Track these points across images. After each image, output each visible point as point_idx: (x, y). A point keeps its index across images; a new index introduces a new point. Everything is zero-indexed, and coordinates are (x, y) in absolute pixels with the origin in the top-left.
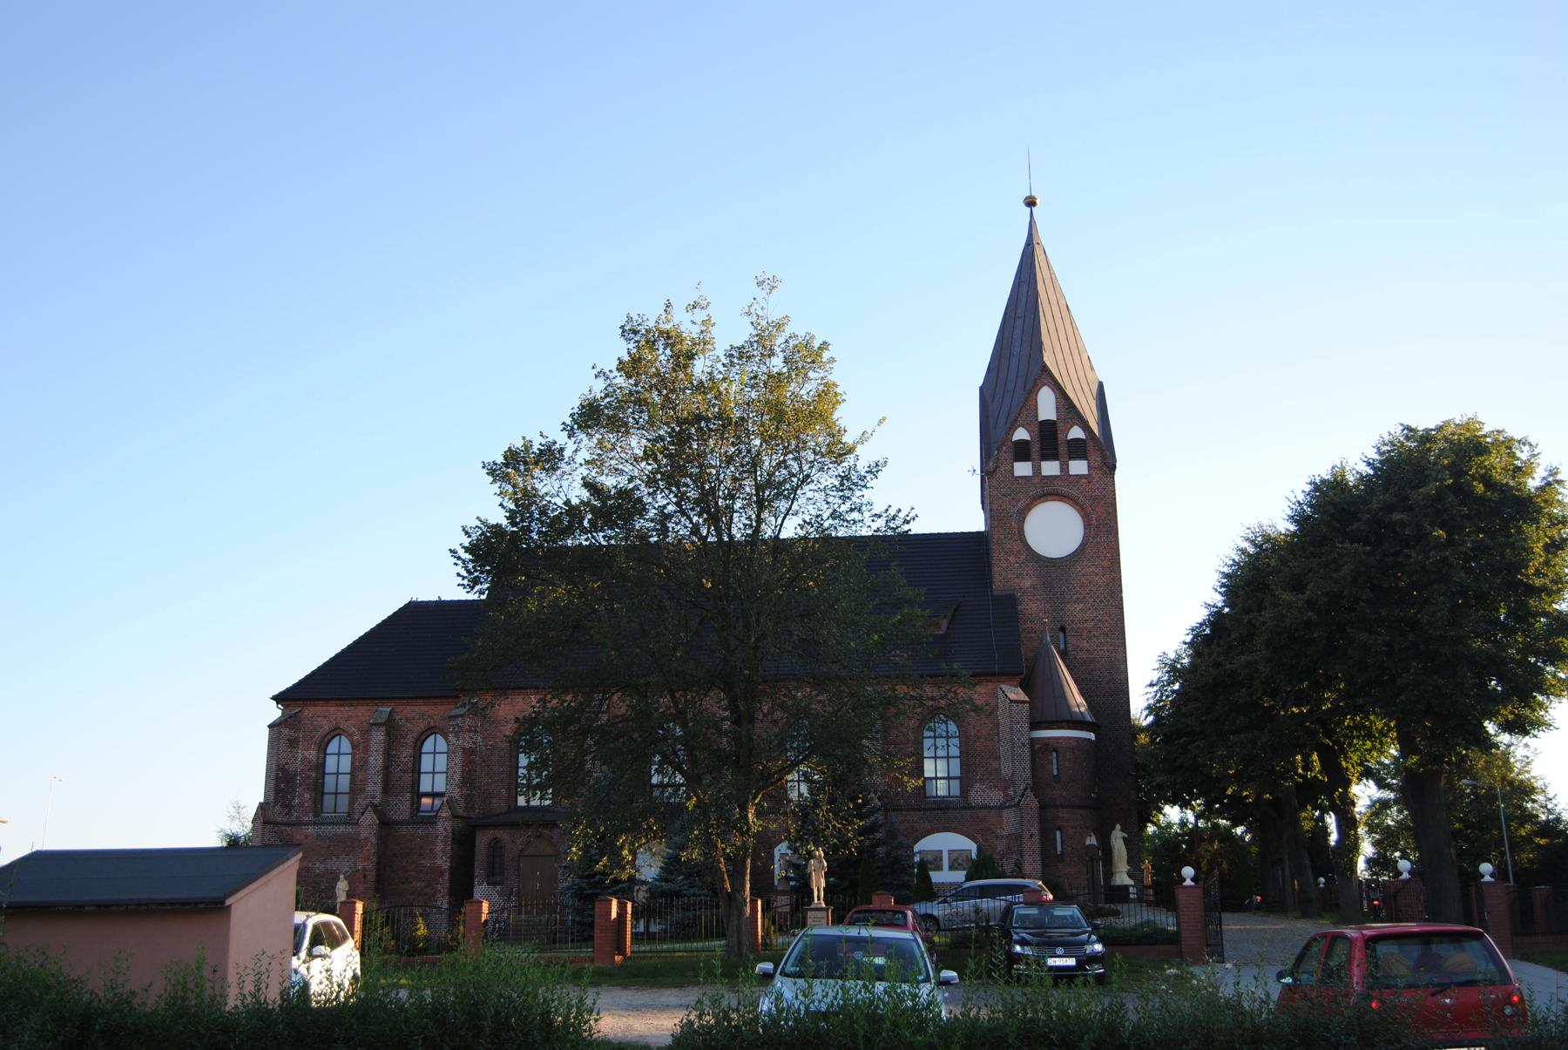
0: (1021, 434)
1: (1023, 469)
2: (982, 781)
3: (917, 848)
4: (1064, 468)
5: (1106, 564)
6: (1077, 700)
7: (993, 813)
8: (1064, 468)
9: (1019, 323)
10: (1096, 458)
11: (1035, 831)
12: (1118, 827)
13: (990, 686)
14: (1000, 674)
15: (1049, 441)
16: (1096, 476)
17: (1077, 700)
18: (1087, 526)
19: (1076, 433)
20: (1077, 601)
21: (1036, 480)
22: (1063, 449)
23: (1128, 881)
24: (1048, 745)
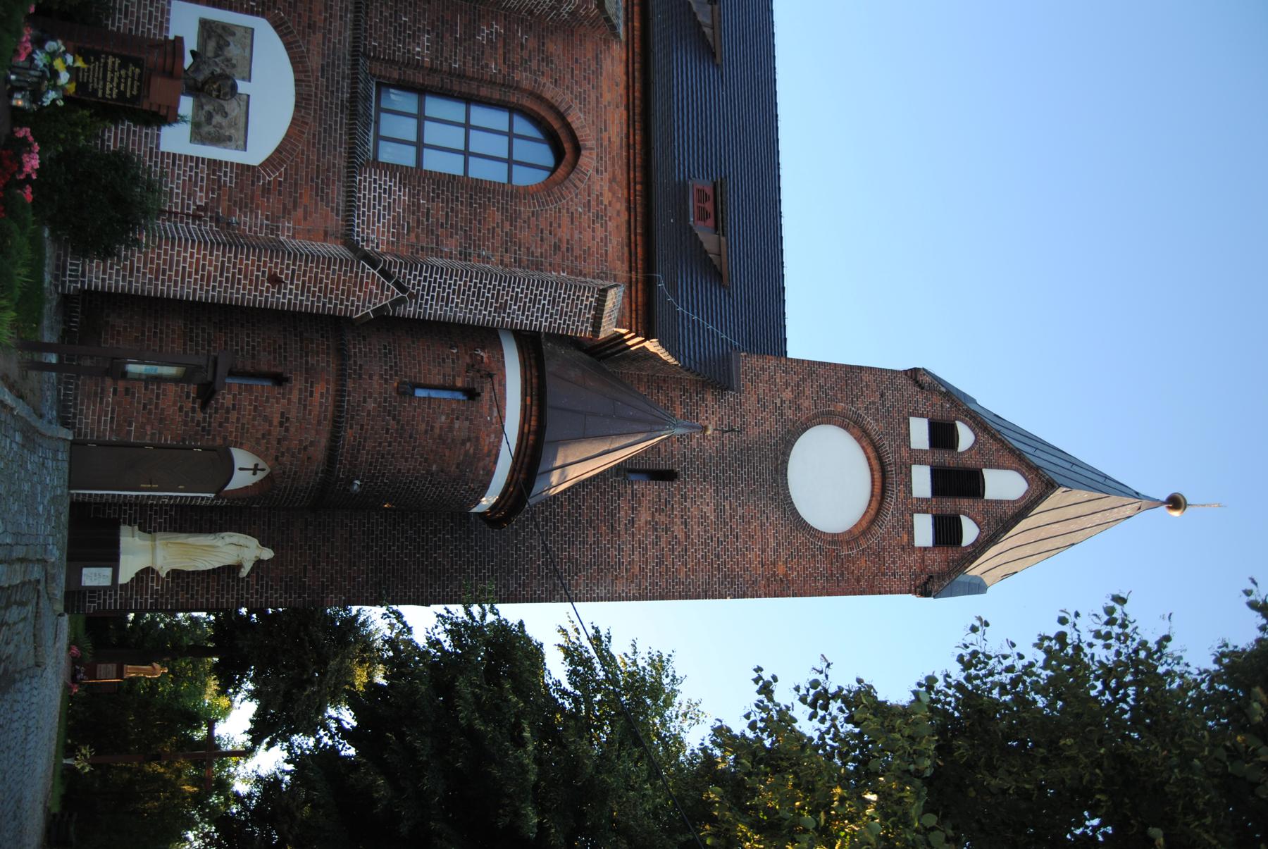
0: (965, 437)
1: (919, 434)
2: (414, 208)
3: (264, 31)
4: (921, 506)
5: (781, 569)
6: (576, 466)
7: (335, 222)
8: (921, 506)
9: (1068, 465)
10: (936, 562)
11: (290, 296)
12: (267, 554)
13: (621, 269)
14: (649, 283)
15: (958, 483)
16: (912, 560)
17: (576, 466)
18: (835, 539)
19: (970, 531)
20: (719, 510)
21: (905, 454)
22: (948, 505)
23: (127, 572)
24: (478, 388)
